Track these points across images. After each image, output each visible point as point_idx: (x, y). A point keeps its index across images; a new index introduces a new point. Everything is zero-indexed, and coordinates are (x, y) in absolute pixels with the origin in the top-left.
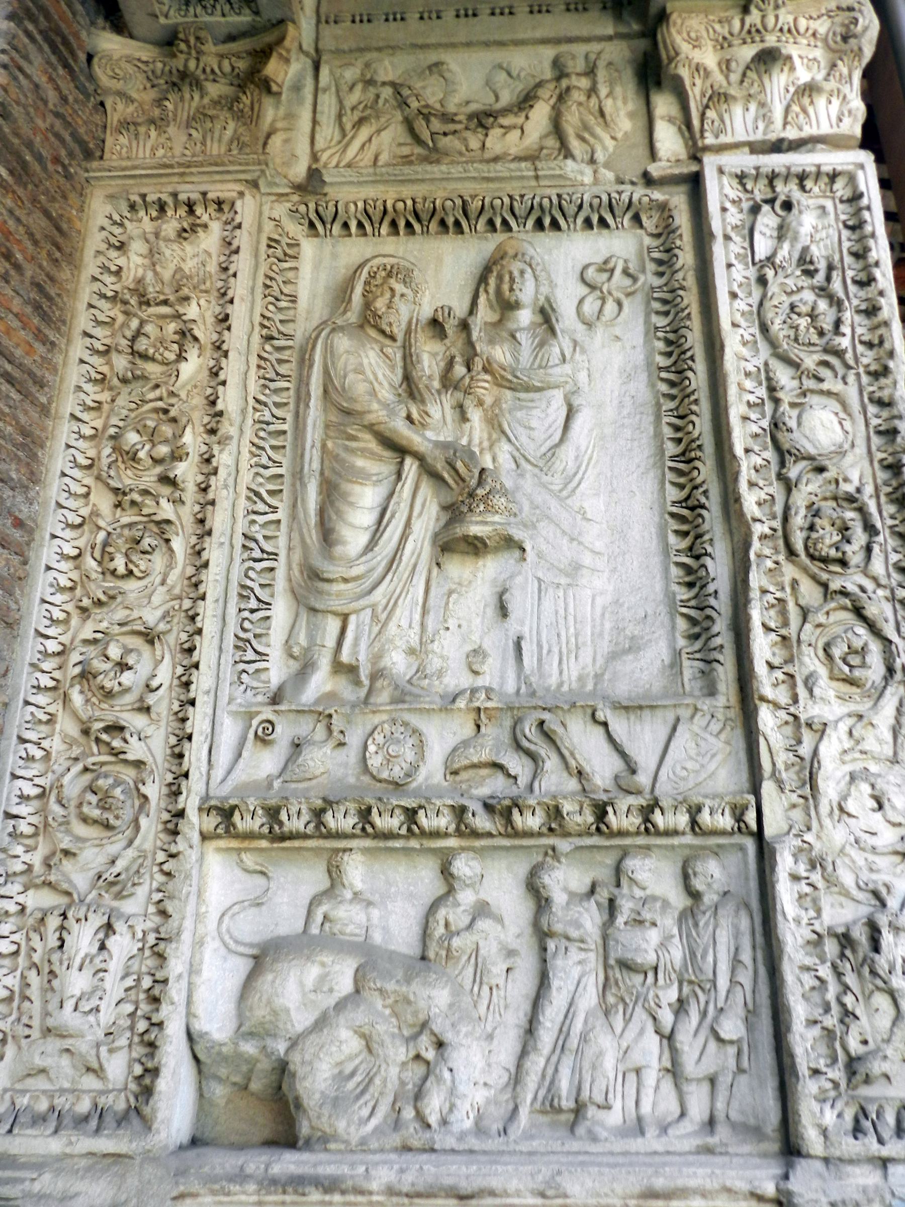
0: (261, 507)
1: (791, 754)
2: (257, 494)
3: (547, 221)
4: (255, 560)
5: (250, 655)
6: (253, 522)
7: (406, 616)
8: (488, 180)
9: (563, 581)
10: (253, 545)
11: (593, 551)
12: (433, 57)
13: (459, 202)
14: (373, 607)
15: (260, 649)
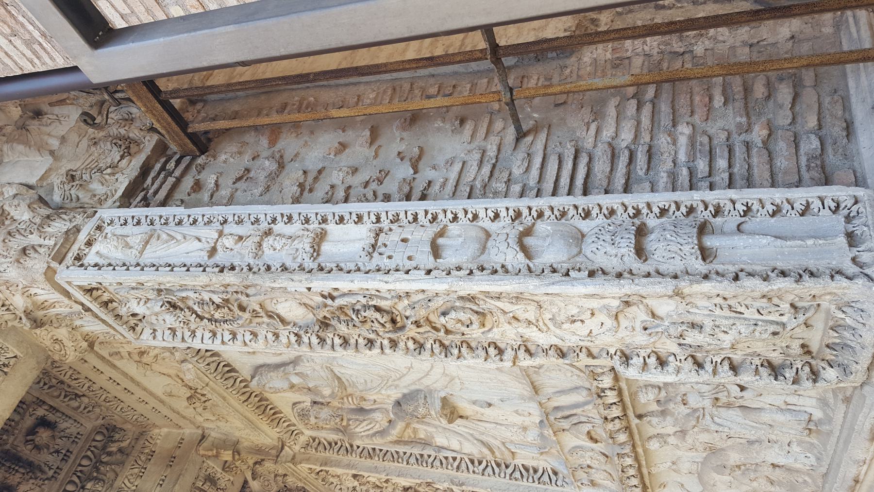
0: (463, 466)
1: (550, 352)
2: (458, 468)
3: (227, 369)
4: (494, 473)
5: (546, 478)
6: (474, 472)
7: (507, 434)
8: (224, 398)
9: (457, 381)
10: (486, 473)
11: (432, 366)
12: (163, 397)
13: (246, 403)
14: (503, 443)
15: (541, 471)
